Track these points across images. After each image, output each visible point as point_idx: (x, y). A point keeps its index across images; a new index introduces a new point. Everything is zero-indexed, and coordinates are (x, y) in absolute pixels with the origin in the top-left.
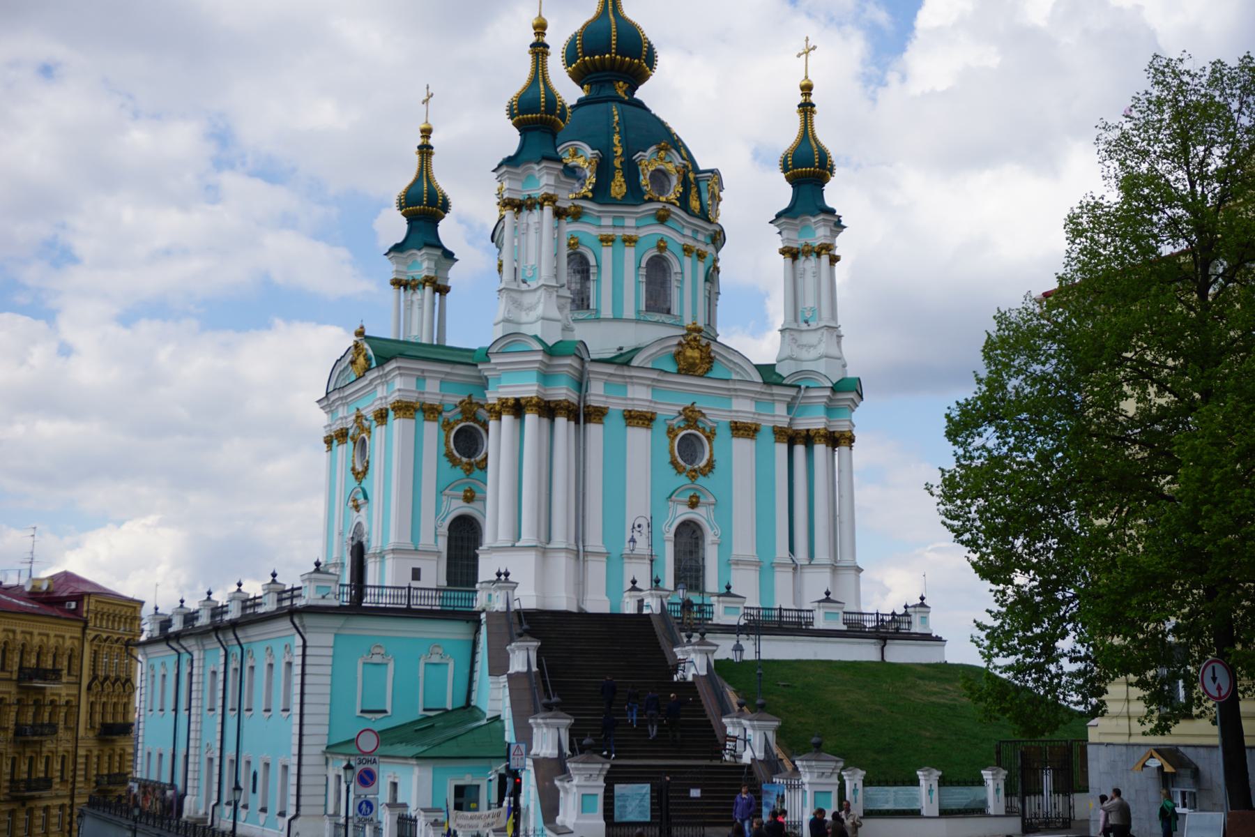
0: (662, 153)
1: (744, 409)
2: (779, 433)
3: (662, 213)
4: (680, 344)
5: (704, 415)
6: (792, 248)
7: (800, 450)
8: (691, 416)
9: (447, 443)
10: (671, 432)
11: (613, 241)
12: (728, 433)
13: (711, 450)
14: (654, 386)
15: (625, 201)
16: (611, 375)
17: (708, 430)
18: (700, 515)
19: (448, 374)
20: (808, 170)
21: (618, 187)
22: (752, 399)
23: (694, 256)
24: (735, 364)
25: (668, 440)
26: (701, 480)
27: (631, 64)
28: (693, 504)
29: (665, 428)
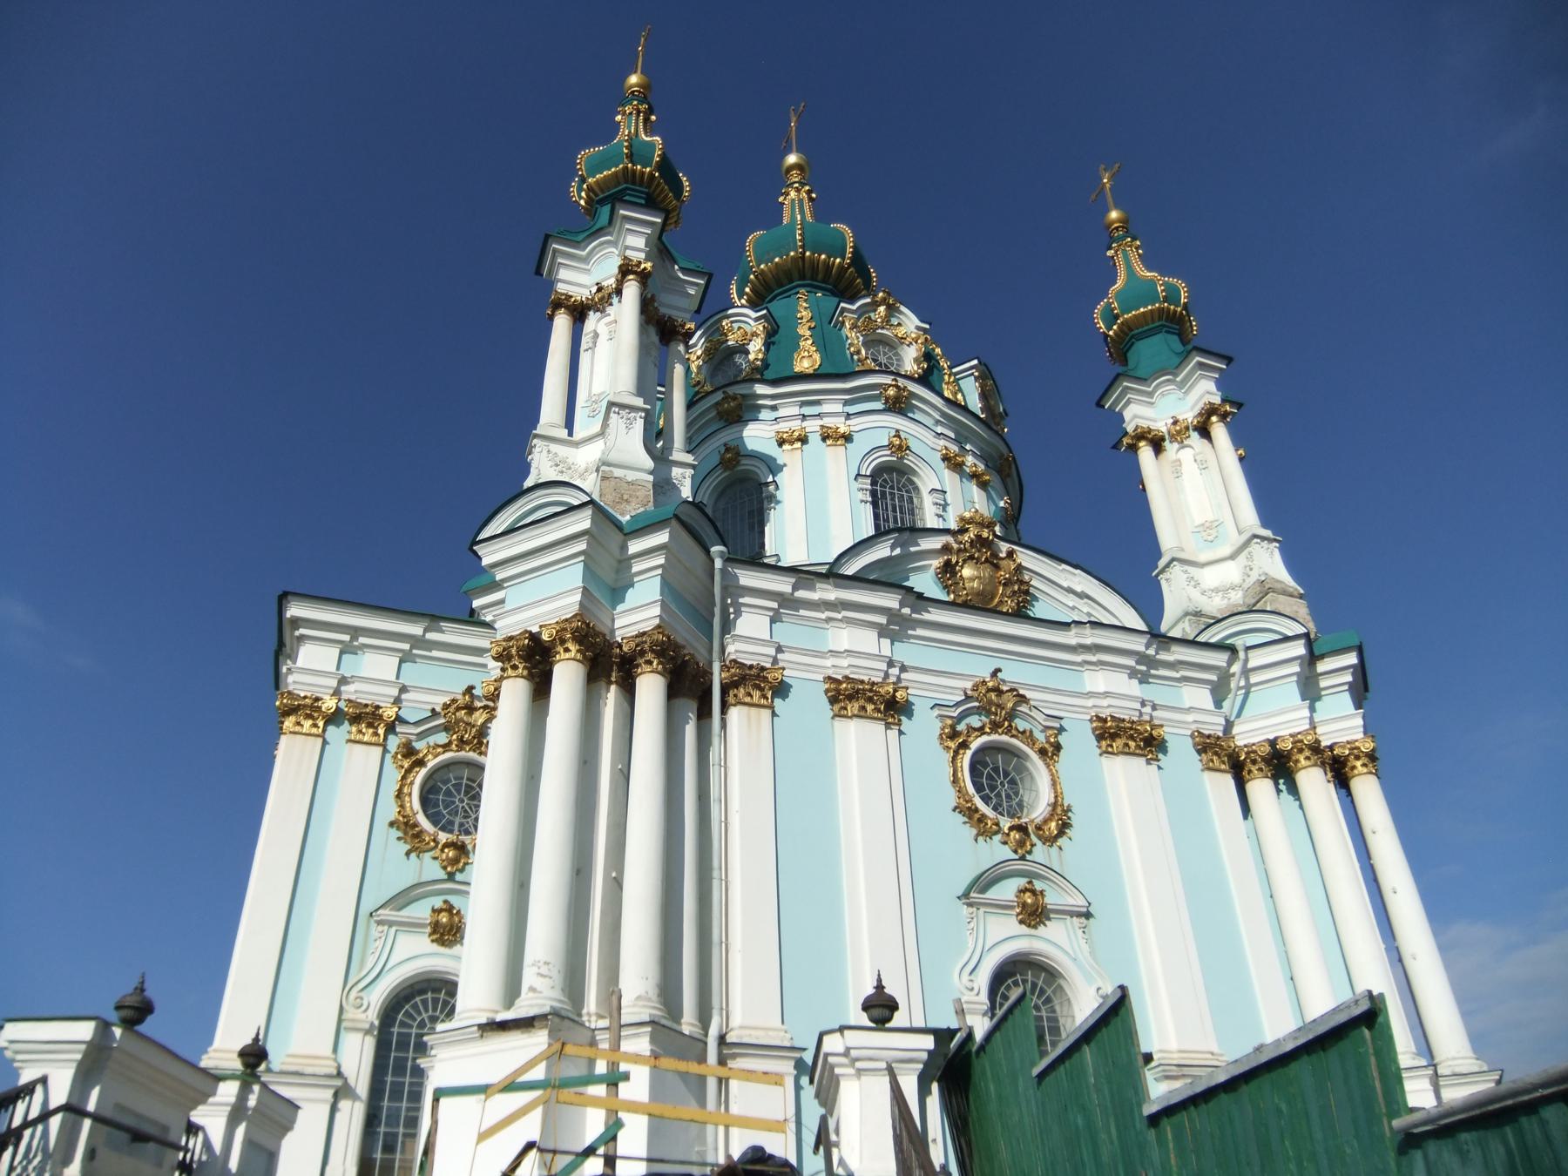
0: (882, 309)
3: (891, 392)
4: (946, 549)
5: (1023, 699)
6: (1150, 430)
8: (996, 703)
9: (399, 795)
11: (803, 440)
13: (1054, 783)
14: (895, 628)
16: (786, 602)
17: (1040, 737)
18: (1055, 942)
19: (417, 642)
21: (806, 362)
22: (1133, 674)
24: (1082, 595)
26: (1040, 852)
27: (828, 267)
29: (936, 727)
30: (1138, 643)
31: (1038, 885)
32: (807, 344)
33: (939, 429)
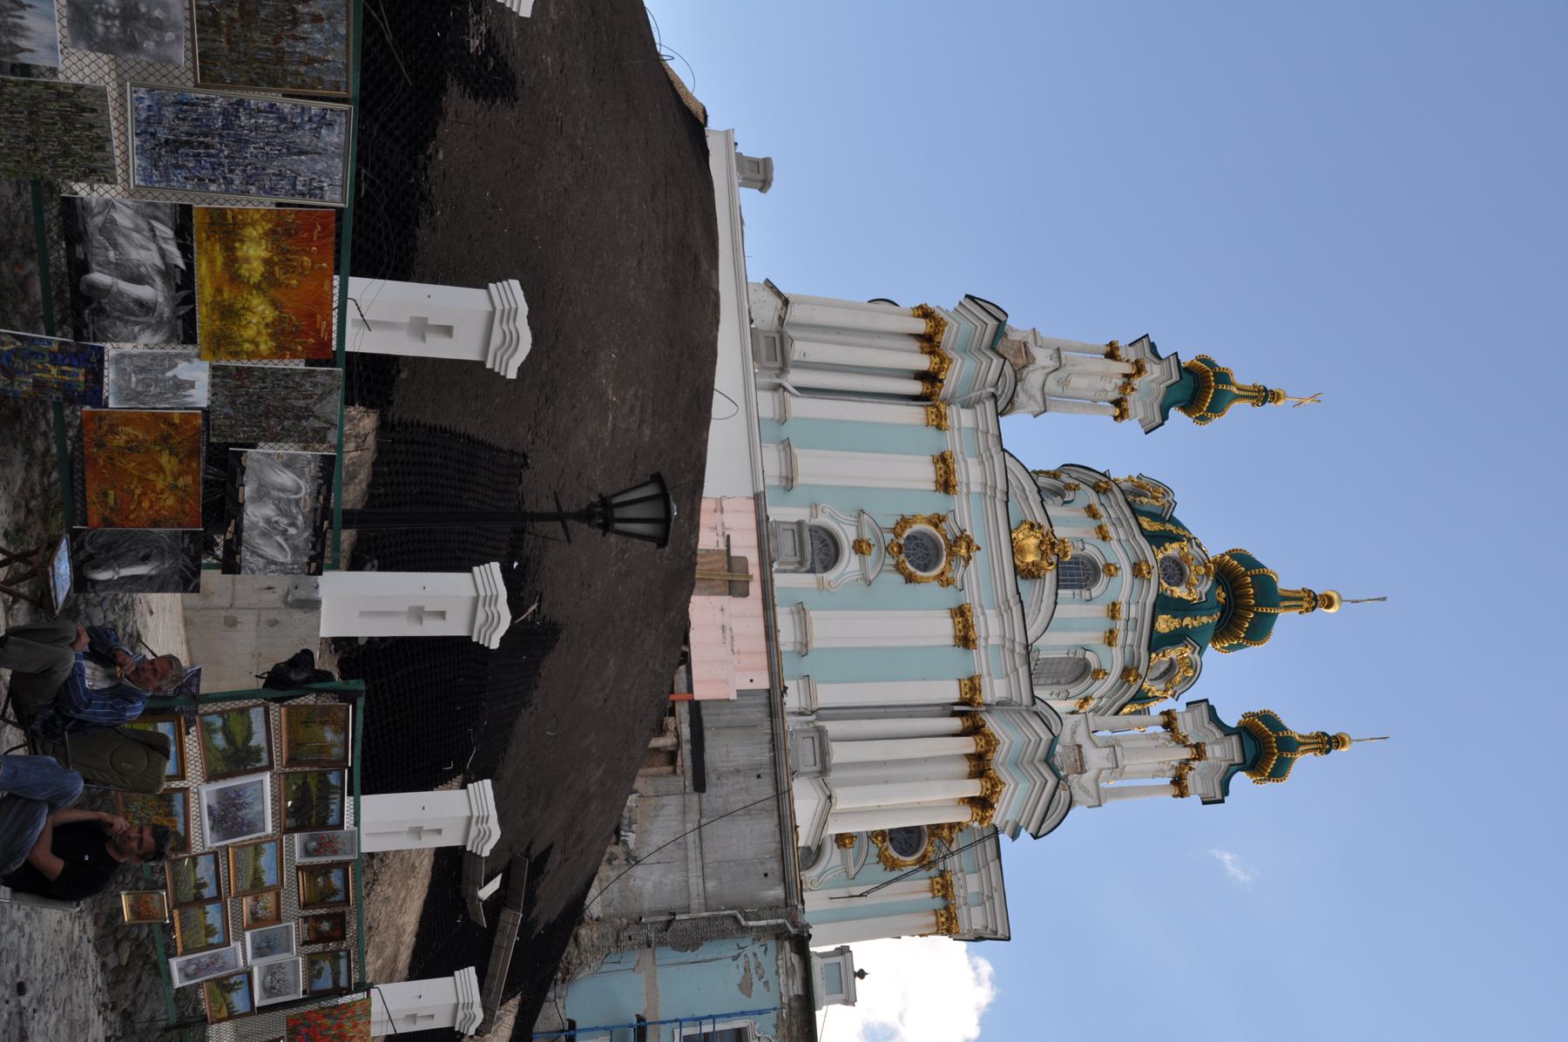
0: (1203, 570)
1: (989, 627)
2: (973, 684)
4: (1040, 527)
7: (956, 724)
8: (961, 545)
10: (937, 521)
12: (954, 605)
14: (988, 488)
15: (1140, 526)
18: (850, 563)
20: (1264, 747)
23: (1108, 624)
25: (928, 513)
26: (890, 561)
28: (859, 547)
30: (1019, 638)
31: (874, 550)
32: (1157, 527)
33: (1133, 607)
